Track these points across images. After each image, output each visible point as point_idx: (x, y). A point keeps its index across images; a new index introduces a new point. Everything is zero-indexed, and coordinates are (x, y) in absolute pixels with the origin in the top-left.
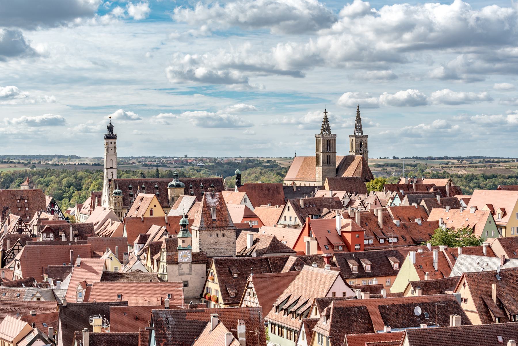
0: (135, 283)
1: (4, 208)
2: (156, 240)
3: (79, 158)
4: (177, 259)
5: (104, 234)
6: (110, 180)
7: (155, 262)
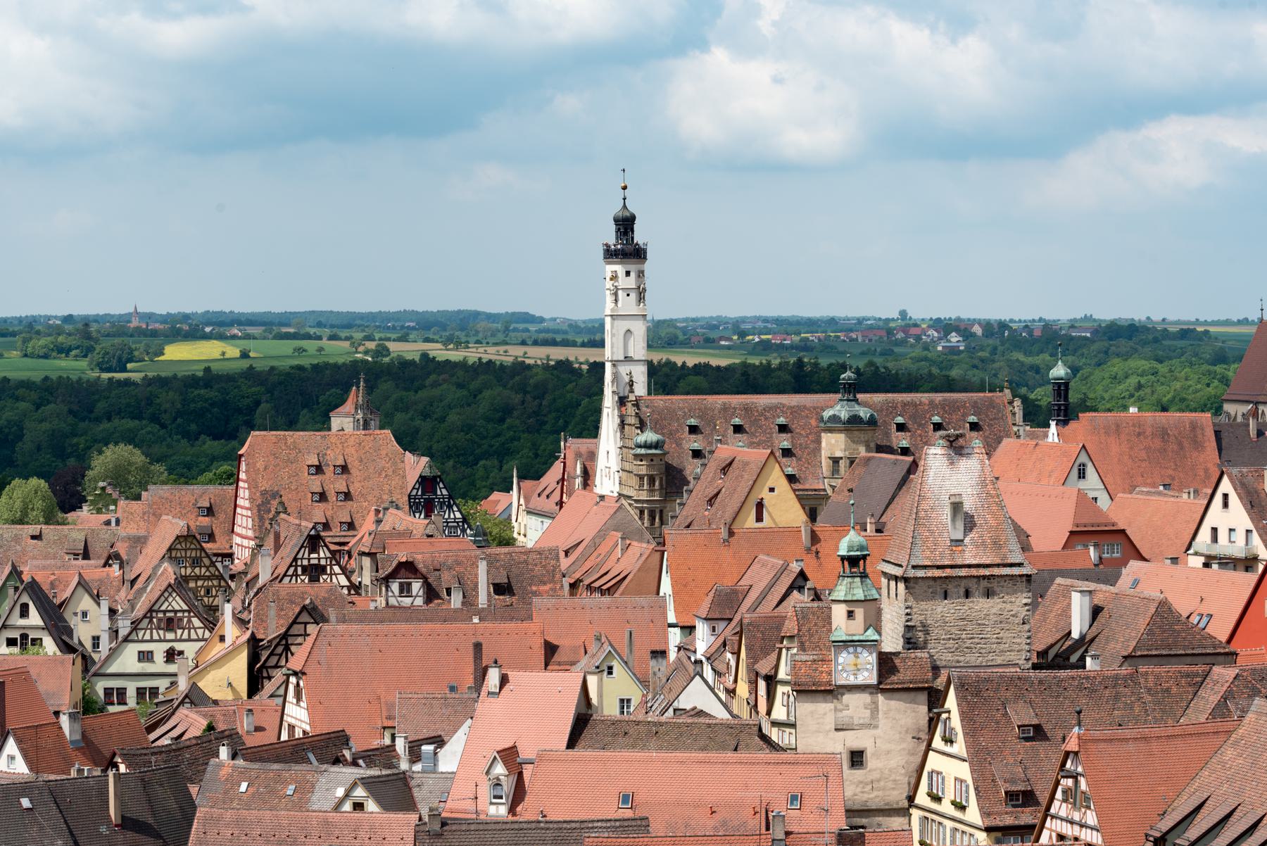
0: (679, 755)
1: (264, 493)
2: (767, 608)
3: (542, 320)
4: (830, 674)
5: (597, 584)
6: (622, 401)
7: (762, 685)
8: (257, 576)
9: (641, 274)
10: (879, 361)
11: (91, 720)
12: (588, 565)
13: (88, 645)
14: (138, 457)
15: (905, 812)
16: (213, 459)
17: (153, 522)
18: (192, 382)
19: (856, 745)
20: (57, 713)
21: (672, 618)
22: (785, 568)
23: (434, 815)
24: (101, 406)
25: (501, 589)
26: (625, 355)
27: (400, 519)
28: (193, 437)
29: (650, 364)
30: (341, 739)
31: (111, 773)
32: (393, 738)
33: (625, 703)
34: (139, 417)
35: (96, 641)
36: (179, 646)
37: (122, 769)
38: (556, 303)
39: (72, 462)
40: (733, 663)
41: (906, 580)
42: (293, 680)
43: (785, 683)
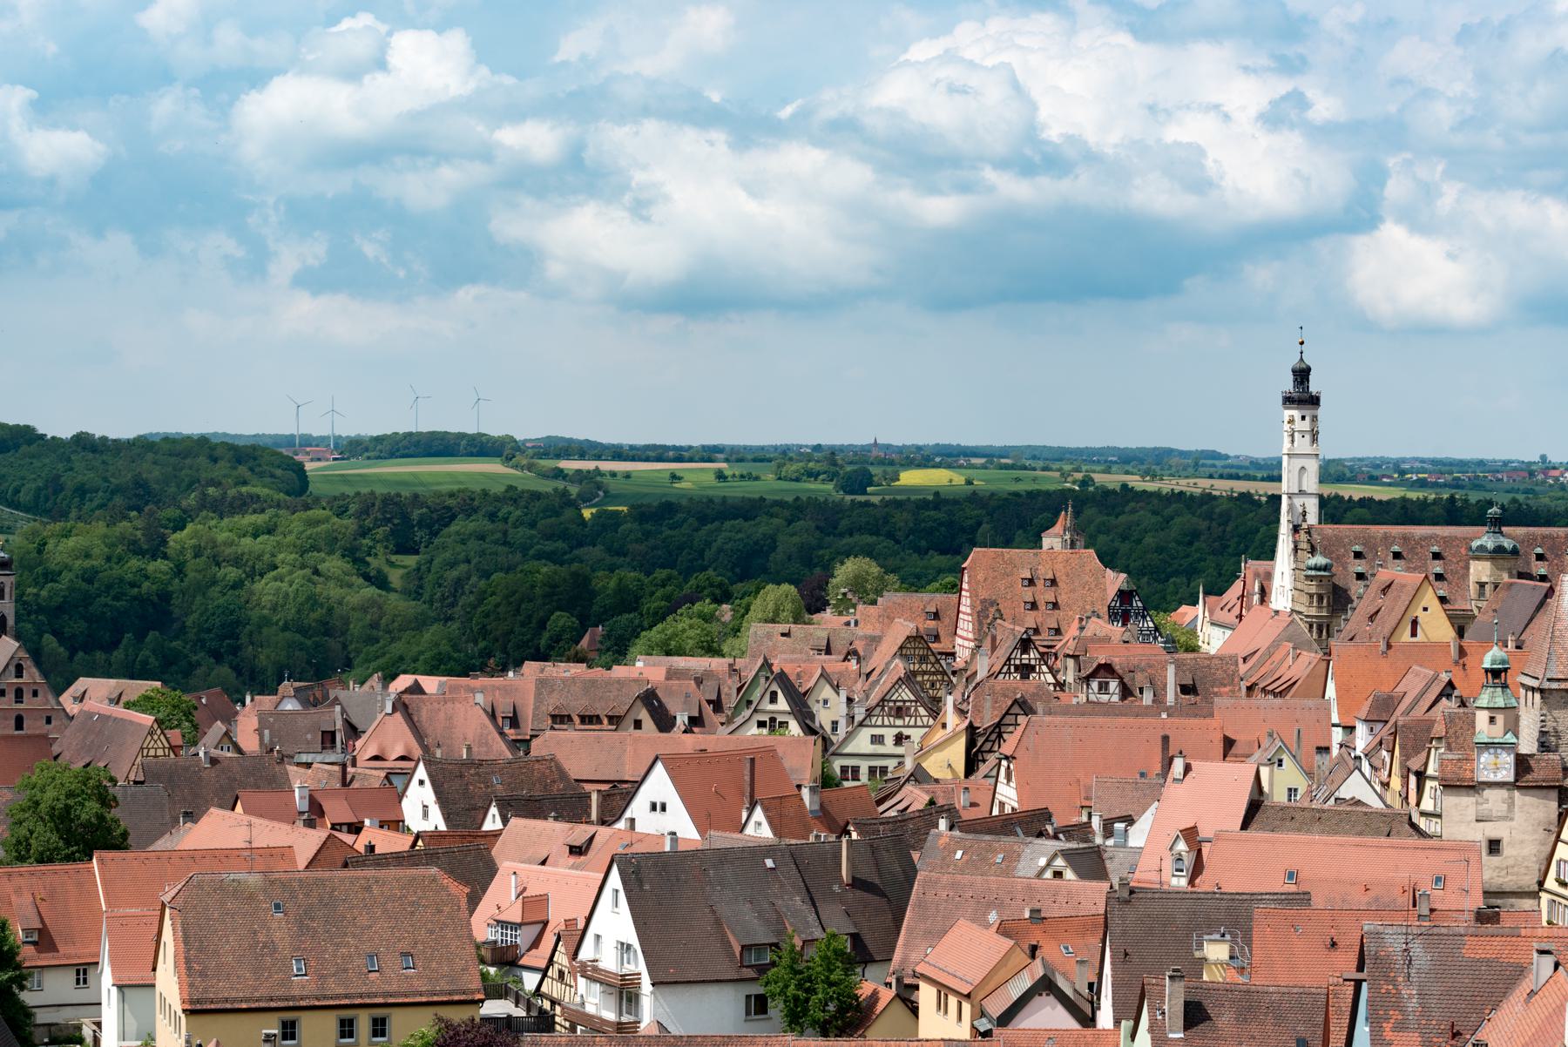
1: (983, 601)
3: (1227, 457)
6: (1296, 529)
7: (1413, 779)
8: (975, 673)
9: (1314, 419)
10: (1521, 497)
11: (830, 794)
12: (1263, 671)
13: (828, 728)
14: (875, 570)
15: (1535, 895)
16: (940, 571)
17: (888, 623)
18: (924, 505)
19: (1494, 835)
20: (799, 787)
21: (1335, 719)
22: (1436, 678)
23: (1124, 884)
24: (844, 523)
25: (1186, 689)
26: (1299, 489)
27: (1101, 627)
28: (922, 552)
29: (1321, 497)
30: (1045, 815)
31: (844, 840)
32: (1090, 816)
33: (1292, 791)
34: (877, 533)
35: (835, 724)
36: (906, 732)
37: (854, 836)
38: (1240, 445)
39: (818, 570)
40: (1388, 760)
41: (1542, 691)
42: (1004, 763)
43: (1433, 778)
